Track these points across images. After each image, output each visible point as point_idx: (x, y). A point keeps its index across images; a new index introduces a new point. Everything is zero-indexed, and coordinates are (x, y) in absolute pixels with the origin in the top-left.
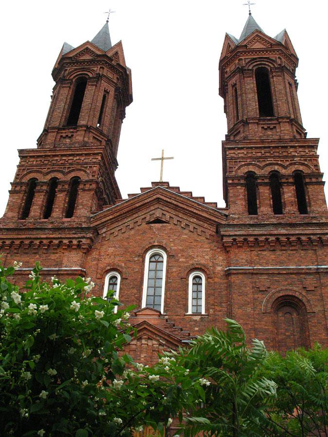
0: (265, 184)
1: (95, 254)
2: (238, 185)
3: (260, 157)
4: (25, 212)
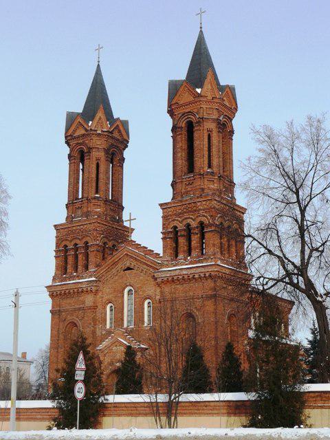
0: (184, 236)
1: (100, 294)
2: (167, 238)
3: (180, 213)
4: (65, 271)
